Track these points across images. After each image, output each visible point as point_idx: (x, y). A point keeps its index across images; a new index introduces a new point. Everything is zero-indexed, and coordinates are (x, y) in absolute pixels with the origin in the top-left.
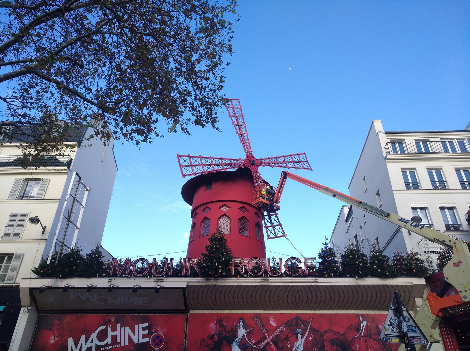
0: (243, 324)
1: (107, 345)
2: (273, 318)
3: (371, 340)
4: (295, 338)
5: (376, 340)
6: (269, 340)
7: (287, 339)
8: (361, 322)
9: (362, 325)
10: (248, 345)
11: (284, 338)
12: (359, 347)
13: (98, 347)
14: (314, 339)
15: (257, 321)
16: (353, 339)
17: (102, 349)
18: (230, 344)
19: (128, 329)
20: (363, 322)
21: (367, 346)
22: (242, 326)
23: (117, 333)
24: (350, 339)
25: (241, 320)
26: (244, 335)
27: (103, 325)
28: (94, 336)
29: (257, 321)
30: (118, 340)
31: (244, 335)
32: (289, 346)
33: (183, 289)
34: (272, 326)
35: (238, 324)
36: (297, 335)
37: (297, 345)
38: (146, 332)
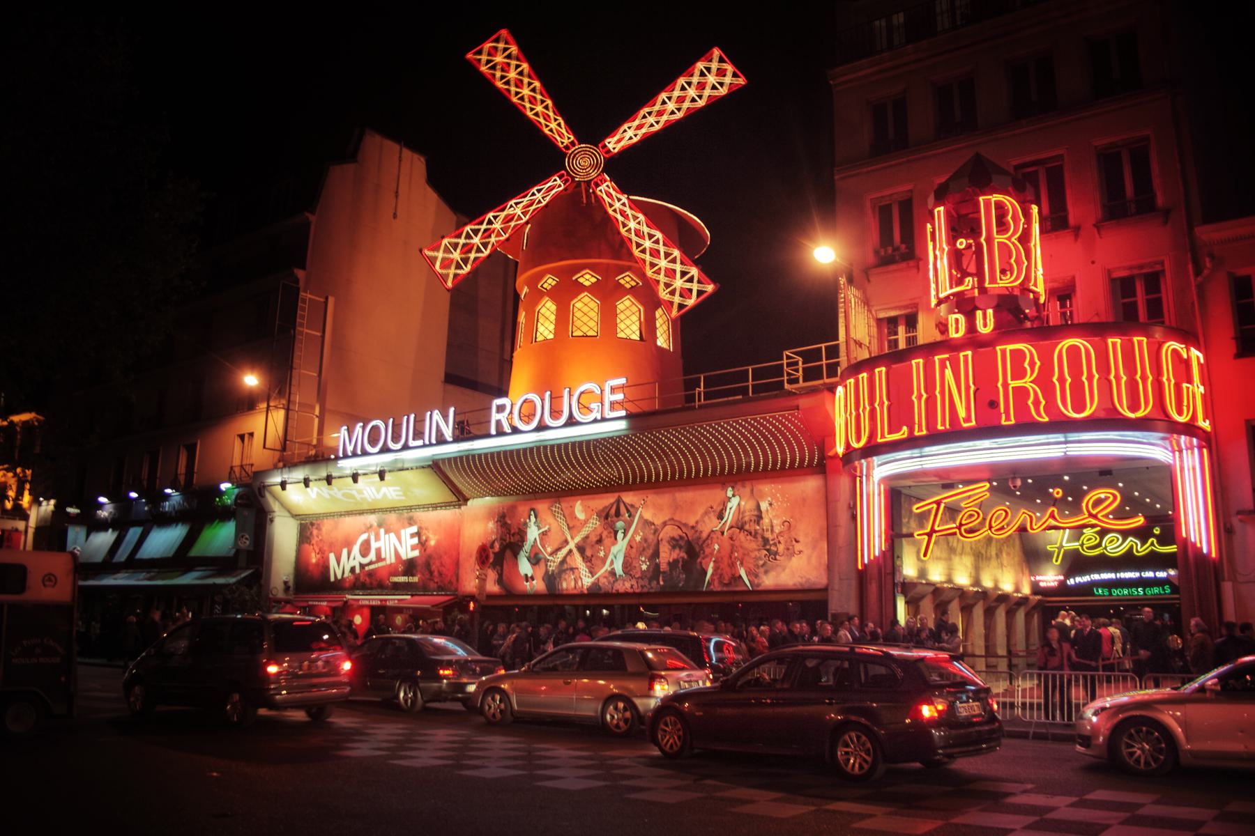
0: (535, 519)
1: (371, 563)
2: (581, 504)
3: (742, 533)
4: (613, 538)
5: (751, 533)
6: (572, 545)
7: (600, 541)
8: (729, 499)
9: (729, 505)
10: (541, 556)
11: (596, 539)
12: (719, 550)
13: (362, 566)
14: (645, 539)
15: (555, 511)
16: (709, 535)
17: (367, 568)
18: (516, 555)
19: (392, 535)
20: (733, 498)
21: (732, 546)
22: (535, 523)
23: (380, 544)
24: (704, 535)
25: (532, 513)
26: (535, 539)
27: (365, 532)
28: (356, 549)
29: (555, 511)
30: (383, 556)
31: (535, 539)
32: (602, 554)
33: (429, 466)
34: (579, 520)
35: (528, 521)
36: (616, 533)
37: (615, 552)
38: (416, 540)
